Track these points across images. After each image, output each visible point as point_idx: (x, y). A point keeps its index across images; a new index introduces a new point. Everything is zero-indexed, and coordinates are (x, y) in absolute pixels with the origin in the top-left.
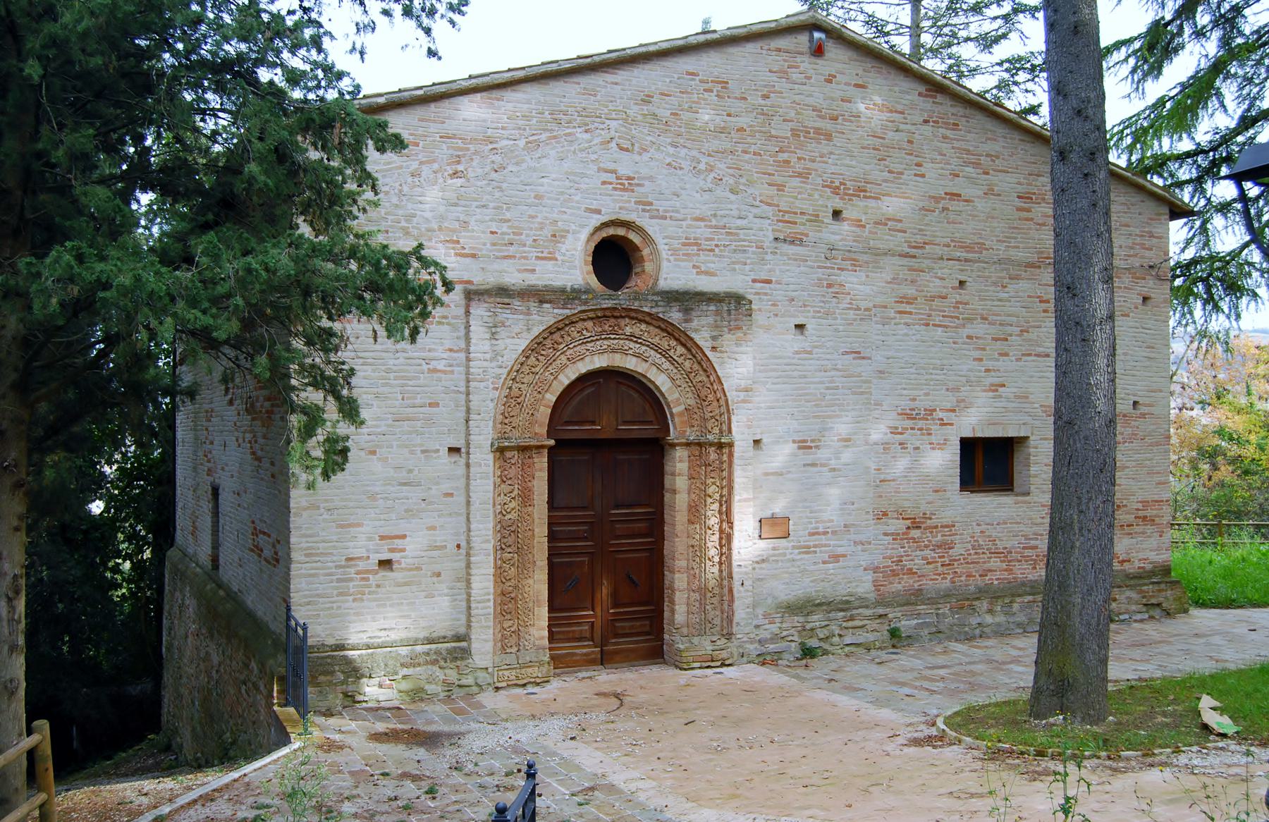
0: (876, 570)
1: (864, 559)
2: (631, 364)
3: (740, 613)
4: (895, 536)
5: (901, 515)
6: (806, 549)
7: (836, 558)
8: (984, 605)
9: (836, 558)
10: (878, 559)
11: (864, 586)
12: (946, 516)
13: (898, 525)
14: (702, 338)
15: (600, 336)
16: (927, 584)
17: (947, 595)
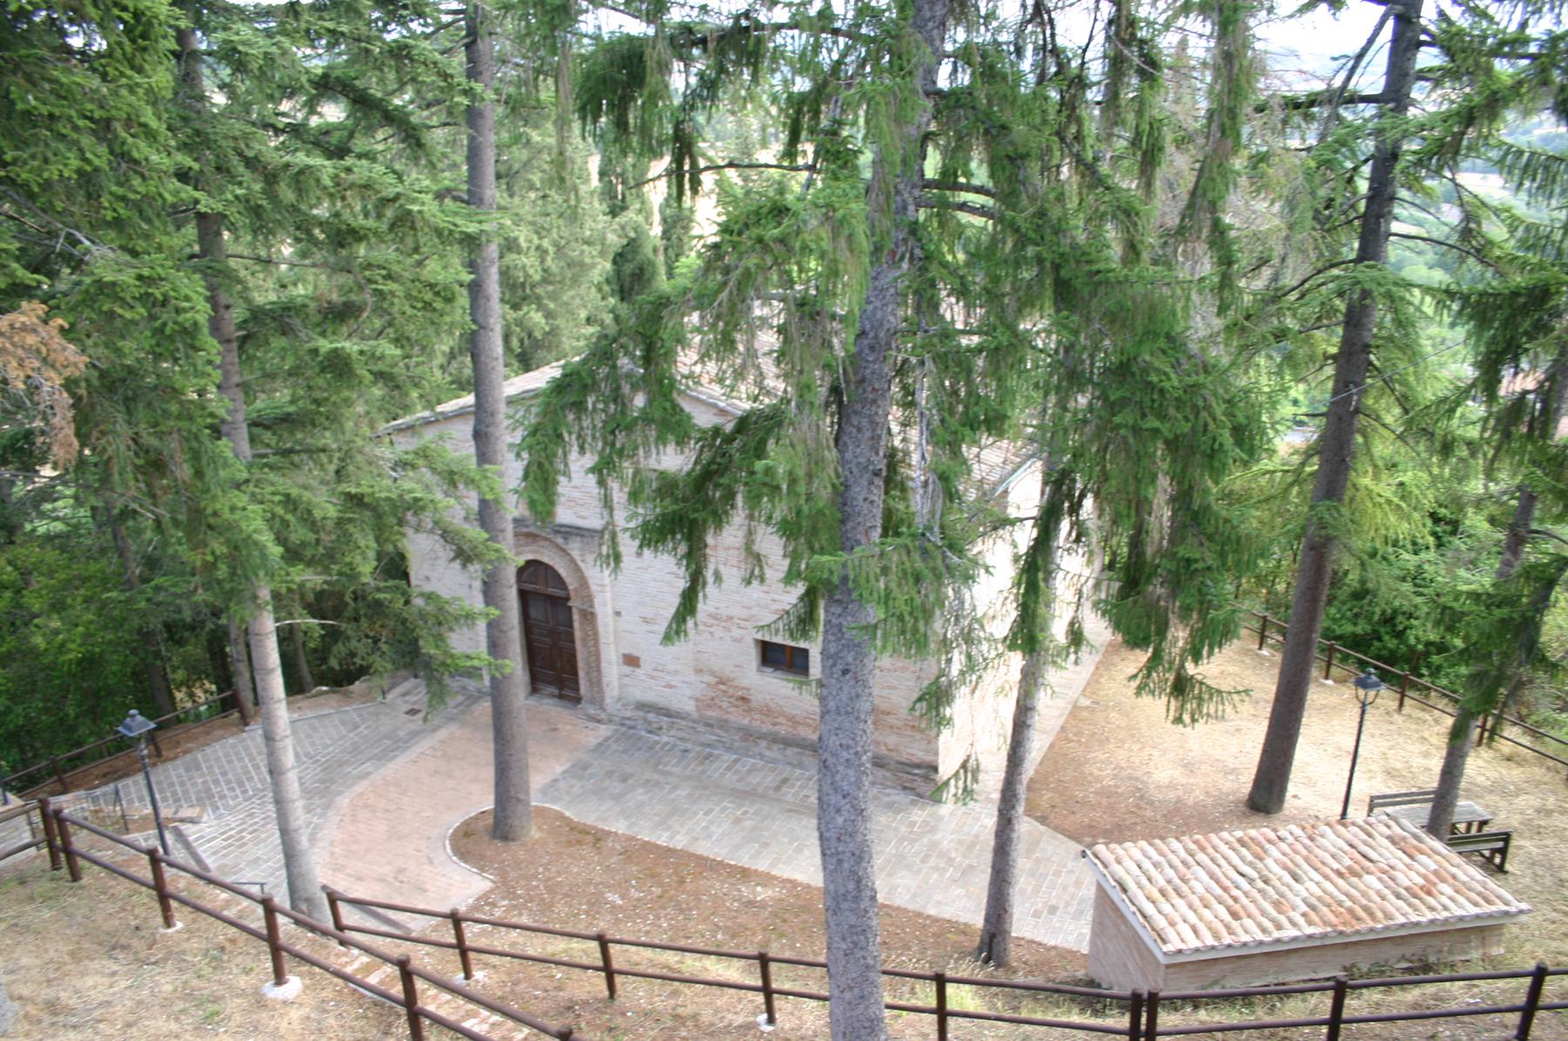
0: (697, 700)
1: (689, 692)
2: (546, 560)
3: (608, 700)
4: (708, 685)
5: (713, 673)
6: (652, 677)
7: (670, 686)
8: (764, 744)
9: (670, 686)
10: (698, 695)
11: (690, 707)
12: (745, 683)
13: (713, 680)
14: (575, 554)
15: (527, 545)
16: (731, 718)
17: (740, 729)
